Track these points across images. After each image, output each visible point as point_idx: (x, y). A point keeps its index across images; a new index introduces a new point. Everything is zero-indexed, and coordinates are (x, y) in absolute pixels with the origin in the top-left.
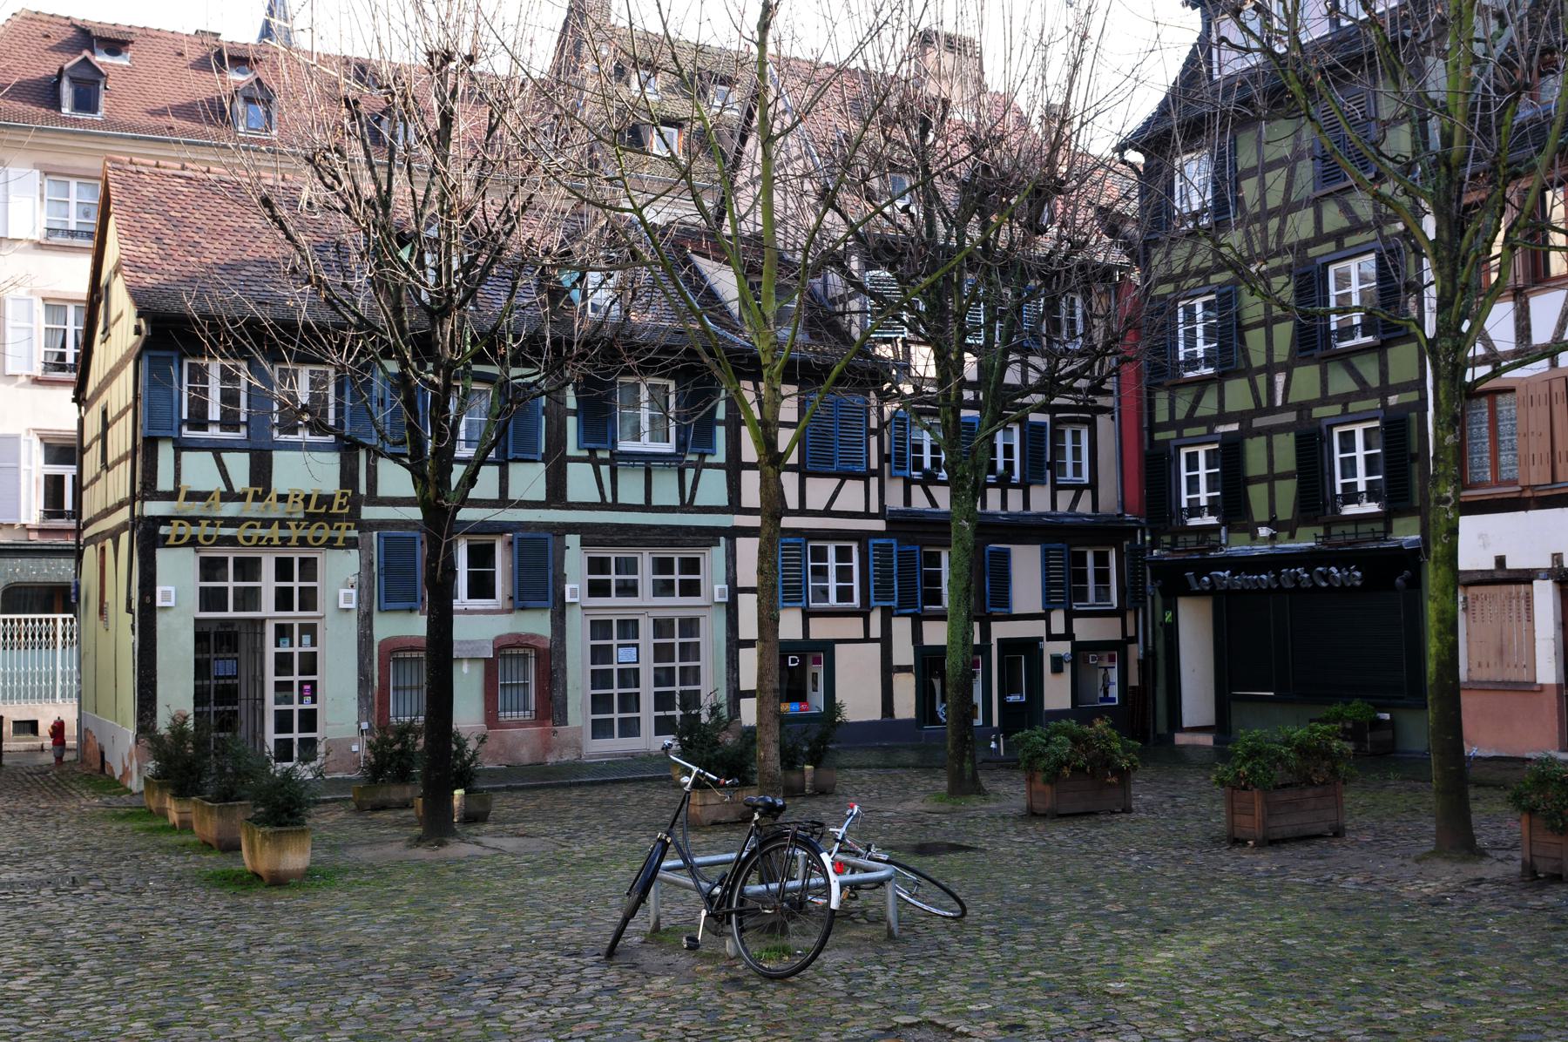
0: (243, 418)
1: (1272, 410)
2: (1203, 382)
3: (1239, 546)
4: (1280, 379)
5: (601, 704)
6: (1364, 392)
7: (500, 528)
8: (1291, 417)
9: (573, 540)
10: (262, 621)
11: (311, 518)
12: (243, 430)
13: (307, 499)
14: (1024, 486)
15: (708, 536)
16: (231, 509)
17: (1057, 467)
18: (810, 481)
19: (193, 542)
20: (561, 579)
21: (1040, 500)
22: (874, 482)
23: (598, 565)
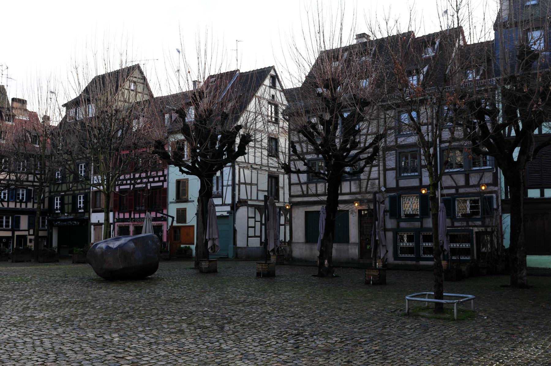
2: (59, 184)
3: (63, 217)
6: (83, 189)
8: (72, 192)
14: (26, 203)
21: (30, 206)
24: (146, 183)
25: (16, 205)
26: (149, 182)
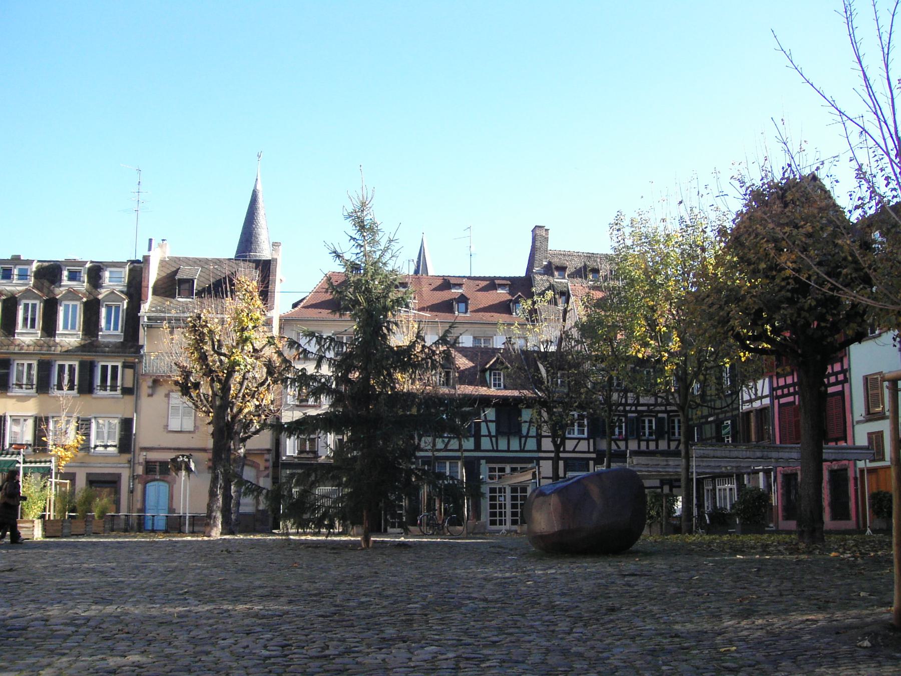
5: (493, 514)
7: (458, 458)
9: (483, 462)
15: (530, 460)
23: (492, 470)
25: (639, 447)
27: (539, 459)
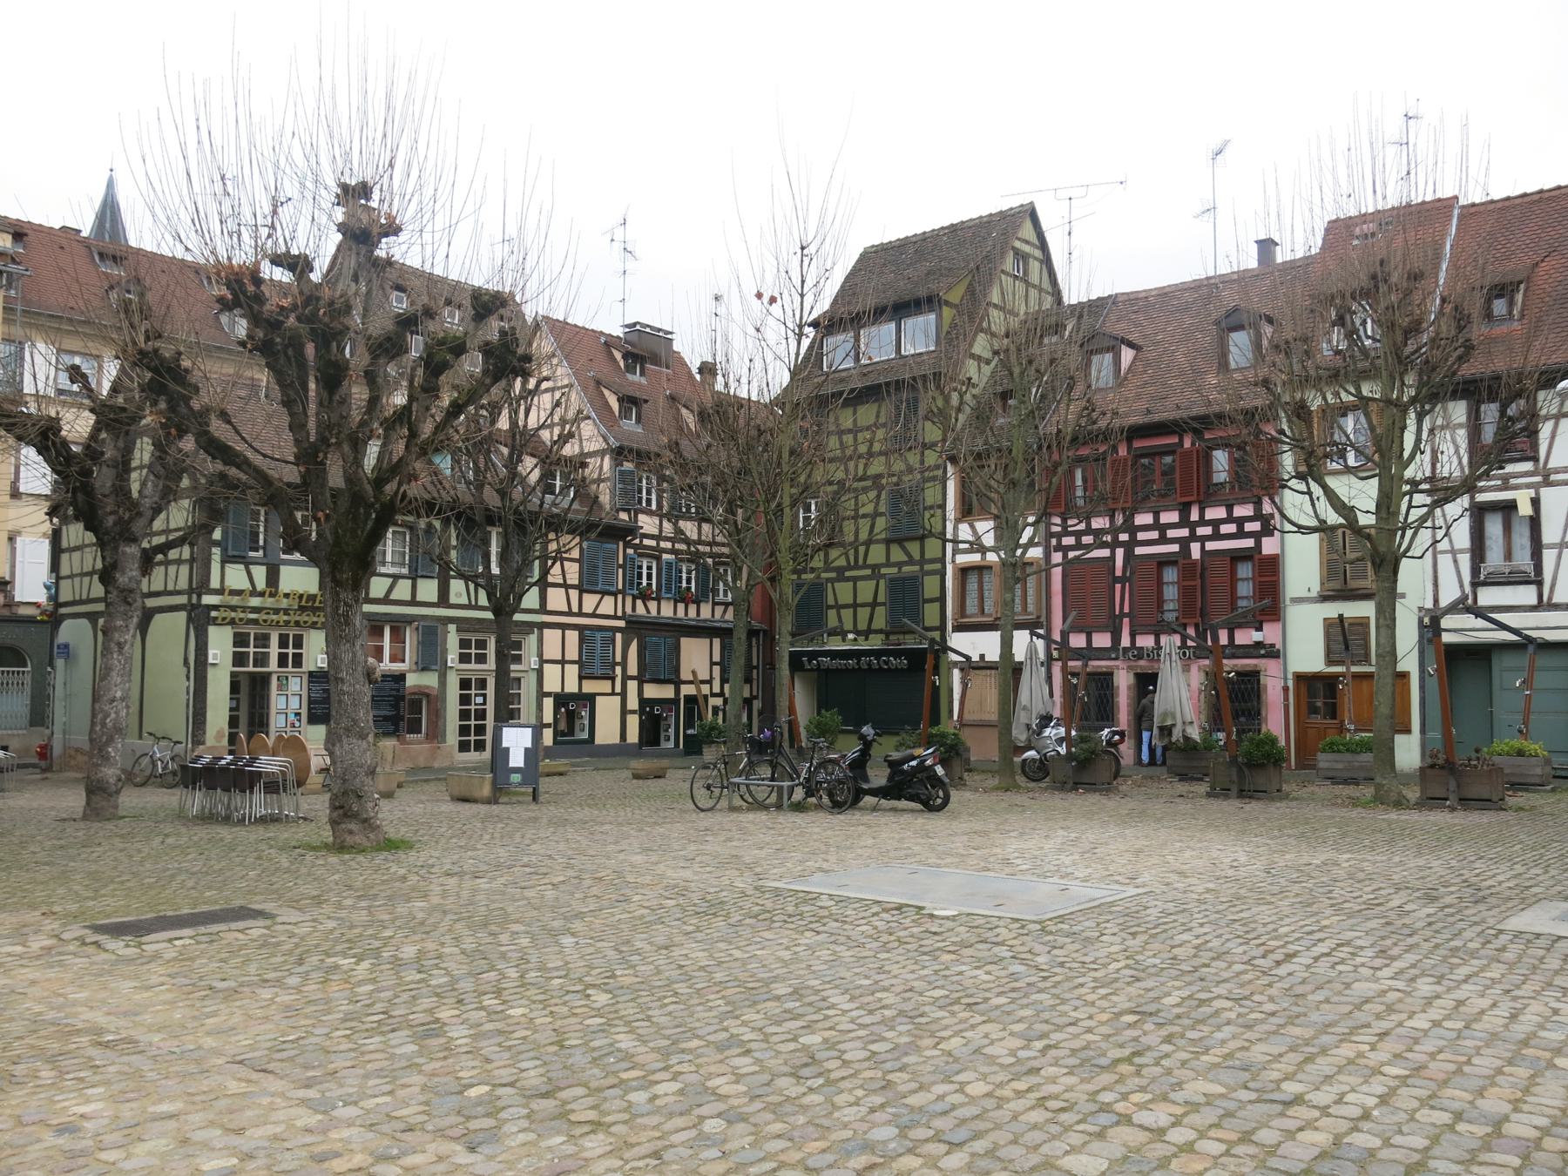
0: (261, 543)
1: (856, 567)
4: (862, 549)
5: (464, 730)
6: (911, 562)
7: (409, 620)
10: (270, 674)
11: (302, 609)
12: (261, 553)
13: (301, 596)
16: (255, 602)
17: (715, 592)
18: (585, 596)
19: (232, 622)
20: (445, 651)
21: (706, 610)
22: (620, 597)
23: (464, 644)
24: (1184, 543)
26: (1193, 537)
27: (543, 626)
